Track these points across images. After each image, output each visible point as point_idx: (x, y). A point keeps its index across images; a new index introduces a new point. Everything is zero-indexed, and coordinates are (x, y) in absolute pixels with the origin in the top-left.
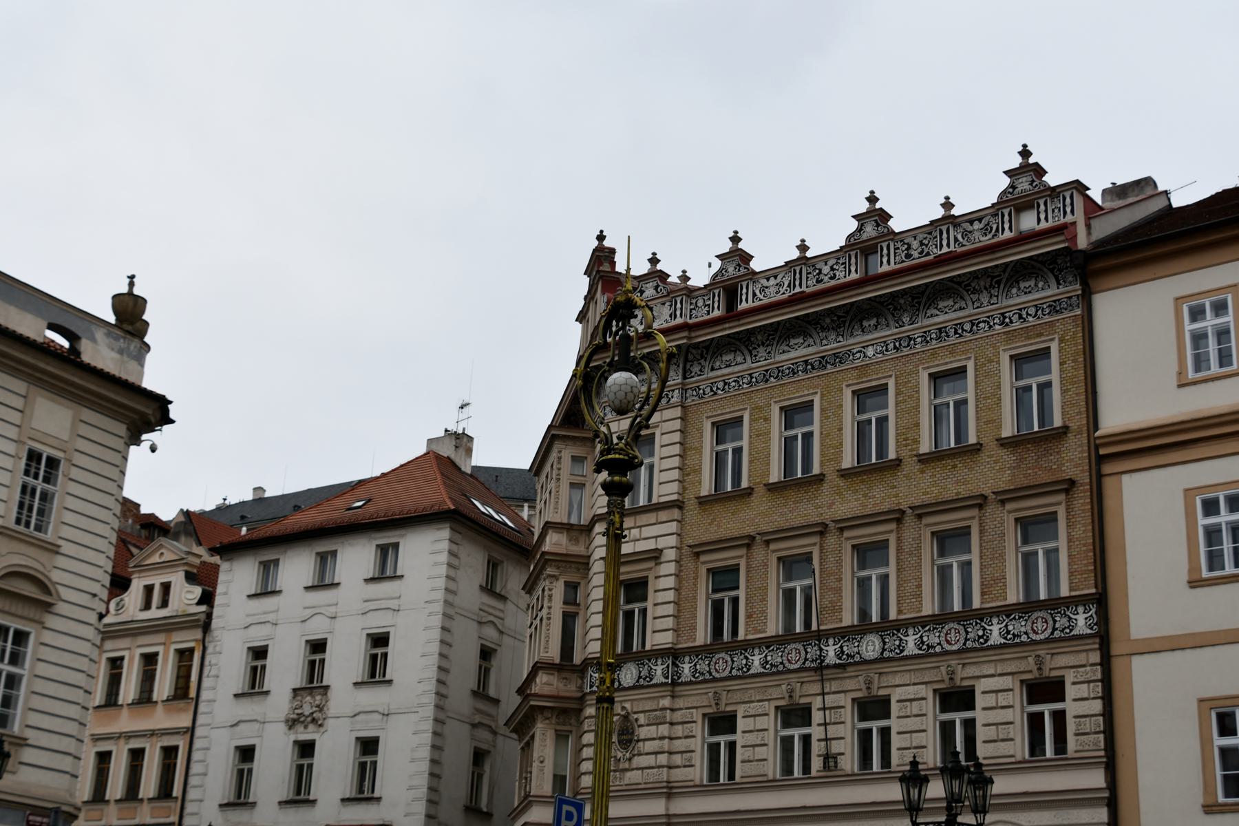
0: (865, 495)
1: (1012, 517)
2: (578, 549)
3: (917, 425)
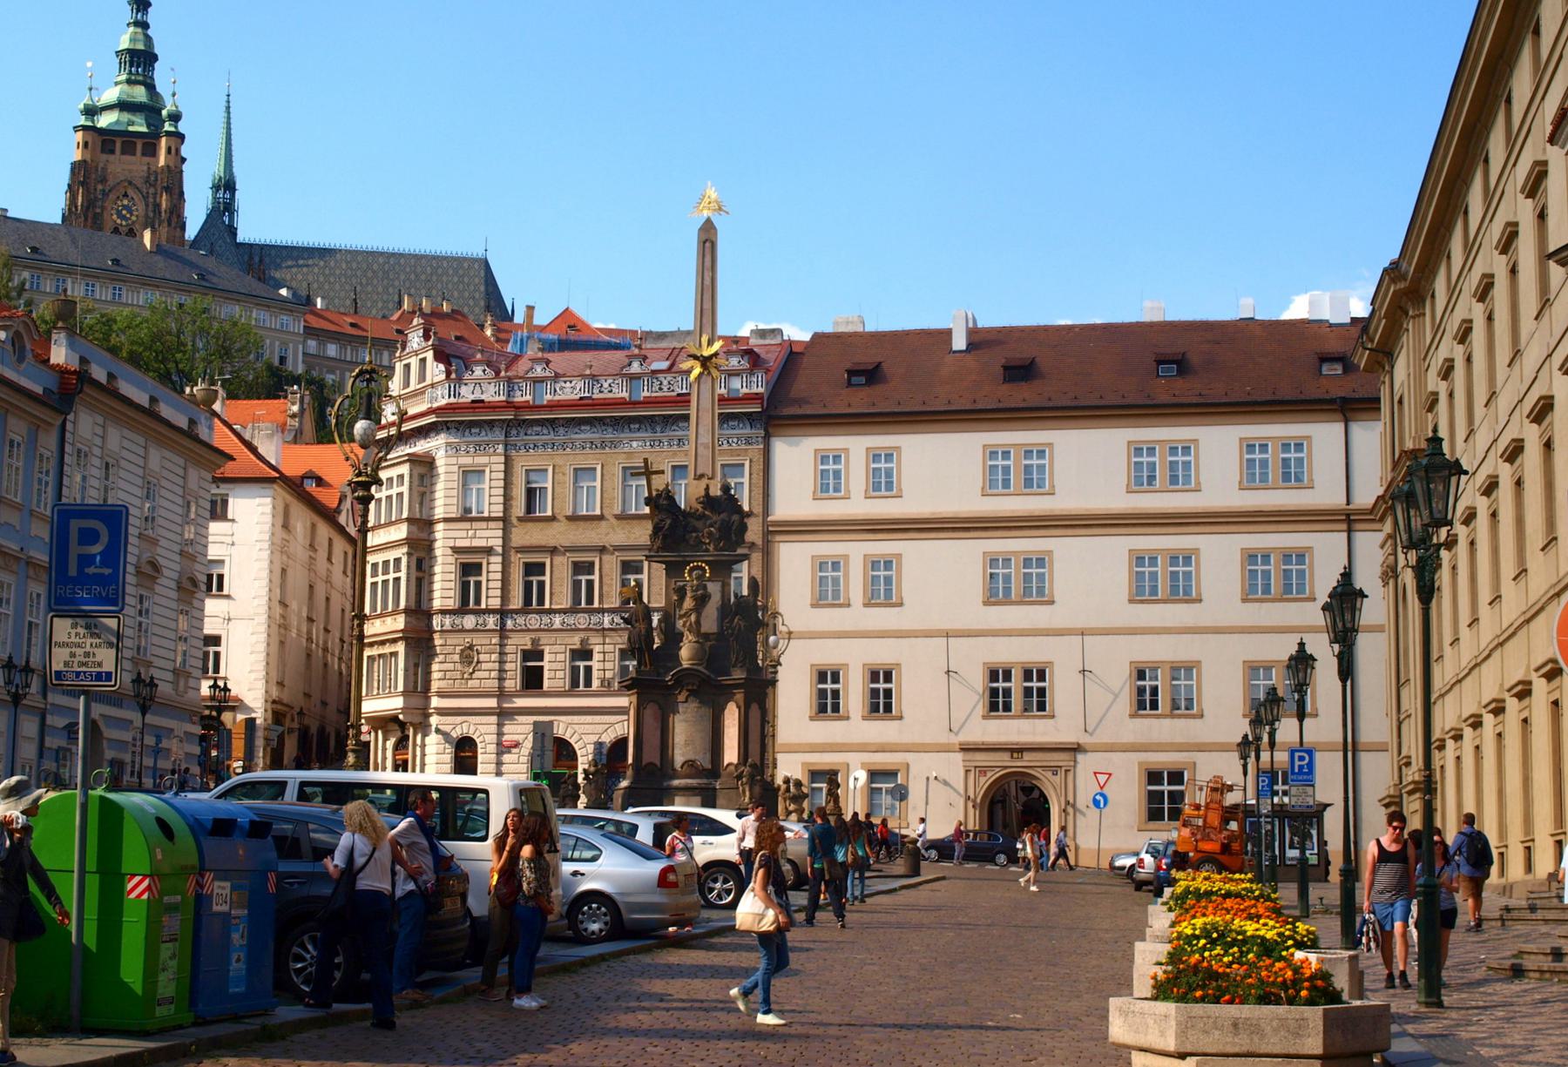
2: (424, 535)
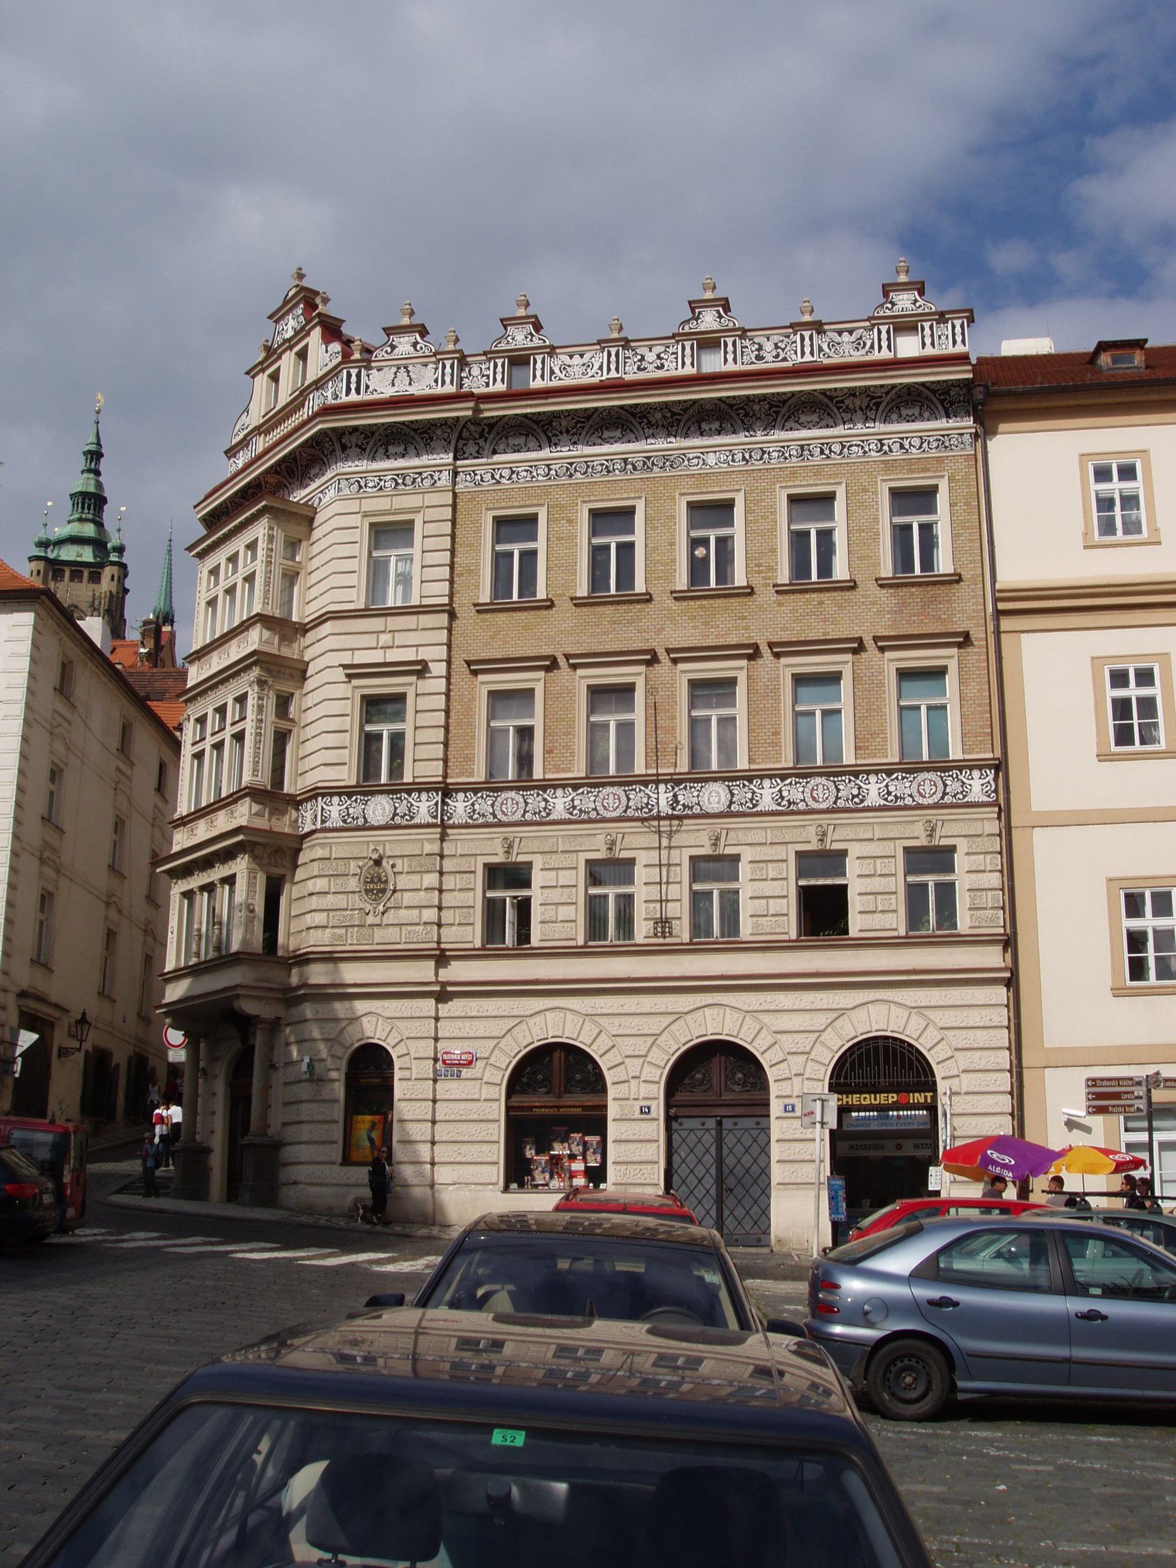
0: (706, 624)
1: (893, 667)
3: (773, 551)
